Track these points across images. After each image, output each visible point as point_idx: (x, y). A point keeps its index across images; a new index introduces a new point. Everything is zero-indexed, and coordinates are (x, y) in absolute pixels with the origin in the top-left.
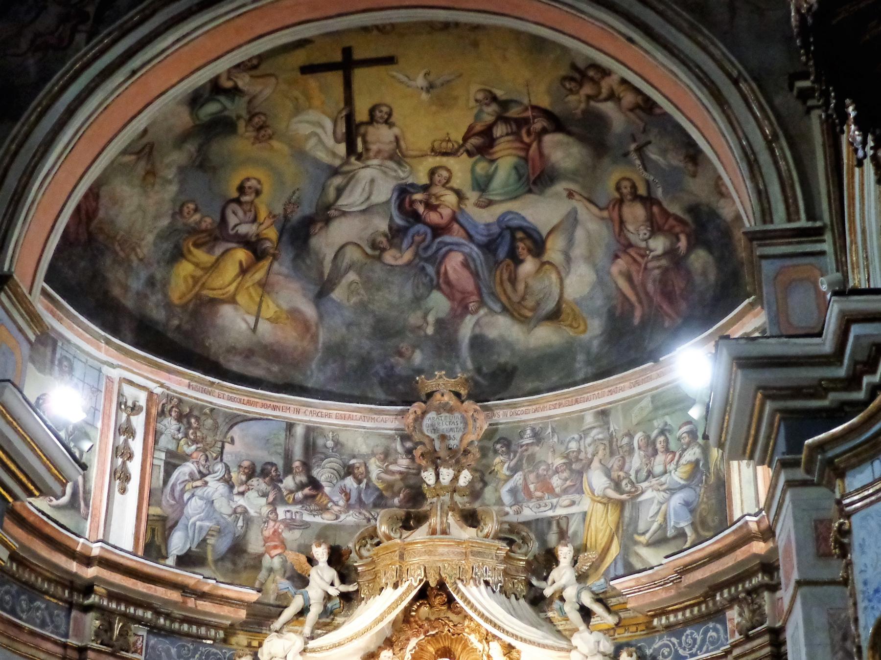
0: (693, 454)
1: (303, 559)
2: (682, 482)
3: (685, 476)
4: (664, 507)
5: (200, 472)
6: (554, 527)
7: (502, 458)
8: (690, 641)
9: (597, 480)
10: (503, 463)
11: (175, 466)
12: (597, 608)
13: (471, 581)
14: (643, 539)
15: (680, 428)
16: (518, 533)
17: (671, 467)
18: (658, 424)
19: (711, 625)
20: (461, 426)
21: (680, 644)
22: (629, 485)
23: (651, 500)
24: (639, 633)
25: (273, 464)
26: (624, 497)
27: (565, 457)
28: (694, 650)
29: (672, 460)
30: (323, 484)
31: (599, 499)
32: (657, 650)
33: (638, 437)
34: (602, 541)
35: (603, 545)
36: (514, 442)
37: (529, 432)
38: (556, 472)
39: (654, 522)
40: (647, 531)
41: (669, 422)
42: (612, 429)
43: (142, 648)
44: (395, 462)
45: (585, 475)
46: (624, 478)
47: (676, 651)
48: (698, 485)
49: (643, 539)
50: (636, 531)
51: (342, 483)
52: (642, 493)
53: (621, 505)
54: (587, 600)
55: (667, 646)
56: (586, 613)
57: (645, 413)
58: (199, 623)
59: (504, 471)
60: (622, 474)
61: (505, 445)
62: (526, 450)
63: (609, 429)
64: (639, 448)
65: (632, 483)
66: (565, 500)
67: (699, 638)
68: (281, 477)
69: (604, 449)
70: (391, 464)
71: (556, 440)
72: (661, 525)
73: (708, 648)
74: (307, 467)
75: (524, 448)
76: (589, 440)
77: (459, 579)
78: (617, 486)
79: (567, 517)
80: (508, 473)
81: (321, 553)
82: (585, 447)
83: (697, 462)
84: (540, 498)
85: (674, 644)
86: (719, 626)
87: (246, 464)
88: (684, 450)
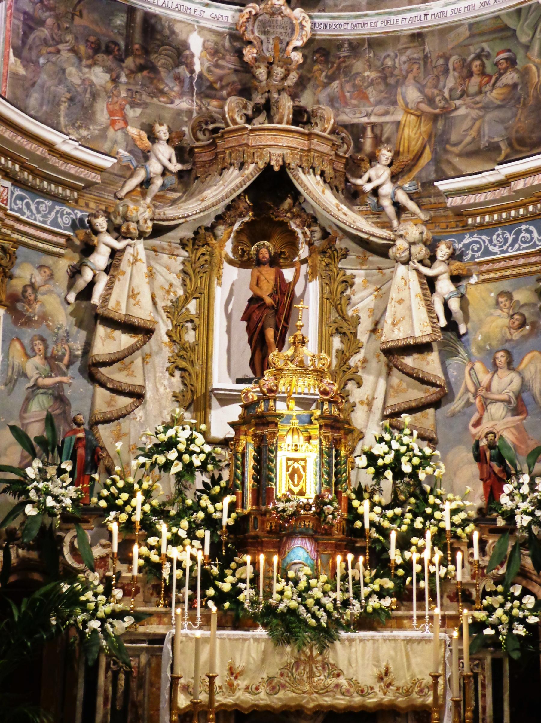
0: (510, 77)
1: (144, 135)
2: (498, 103)
3: (501, 97)
4: (478, 124)
5: (53, 39)
6: (369, 132)
7: (320, 66)
8: (501, 239)
9: (412, 94)
10: (322, 72)
11: (32, 29)
12: (412, 206)
13: (311, 170)
14: (456, 150)
15: (498, 54)
16: (338, 134)
17: (488, 88)
18: (474, 50)
19: (524, 227)
20: (289, 31)
21: (491, 242)
22: (443, 102)
23: (465, 116)
24: (449, 230)
25: (116, 44)
26: (437, 111)
27: (380, 72)
28: (505, 248)
29: (488, 82)
30: (160, 69)
31: (412, 111)
32: (467, 246)
33: (454, 59)
34: (416, 147)
35: (415, 152)
36: (332, 54)
37: (346, 45)
38: (372, 83)
39: (466, 135)
40: (460, 143)
41: (487, 49)
42: (427, 50)
43: (7, 199)
44: (223, 58)
45: (399, 90)
46: (438, 95)
47: (486, 248)
48: (515, 106)
49: (456, 150)
50: (448, 142)
51: (177, 70)
52: (456, 109)
53: (435, 118)
54: (402, 197)
55: (476, 242)
56: (400, 209)
57: (461, 39)
58: (58, 183)
59: (322, 78)
60: (436, 92)
61: (324, 55)
62: (344, 62)
63: (424, 50)
64: (454, 69)
65: (444, 98)
66: (380, 109)
67: (511, 238)
68: (123, 57)
69: (419, 68)
70: (220, 58)
71: (371, 55)
72: (474, 139)
73: (520, 246)
74: (146, 51)
75: (341, 59)
76: (404, 58)
77: (300, 167)
78: (431, 101)
79: (381, 125)
80: (325, 81)
81: (162, 131)
82: (400, 65)
83: (515, 86)
84: (356, 106)
85: (484, 242)
86: (532, 228)
87: (92, 39)
88: (501, 75)
